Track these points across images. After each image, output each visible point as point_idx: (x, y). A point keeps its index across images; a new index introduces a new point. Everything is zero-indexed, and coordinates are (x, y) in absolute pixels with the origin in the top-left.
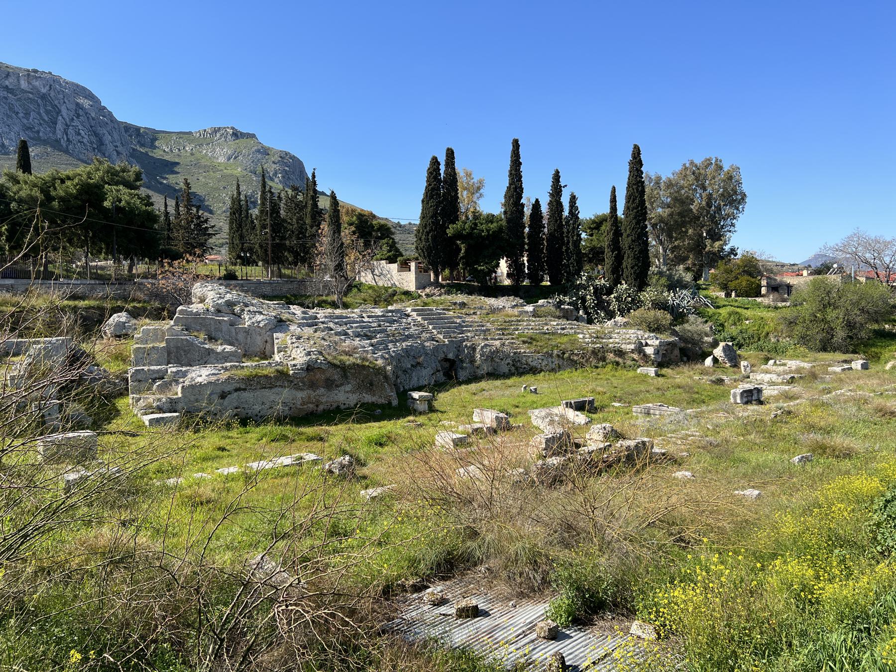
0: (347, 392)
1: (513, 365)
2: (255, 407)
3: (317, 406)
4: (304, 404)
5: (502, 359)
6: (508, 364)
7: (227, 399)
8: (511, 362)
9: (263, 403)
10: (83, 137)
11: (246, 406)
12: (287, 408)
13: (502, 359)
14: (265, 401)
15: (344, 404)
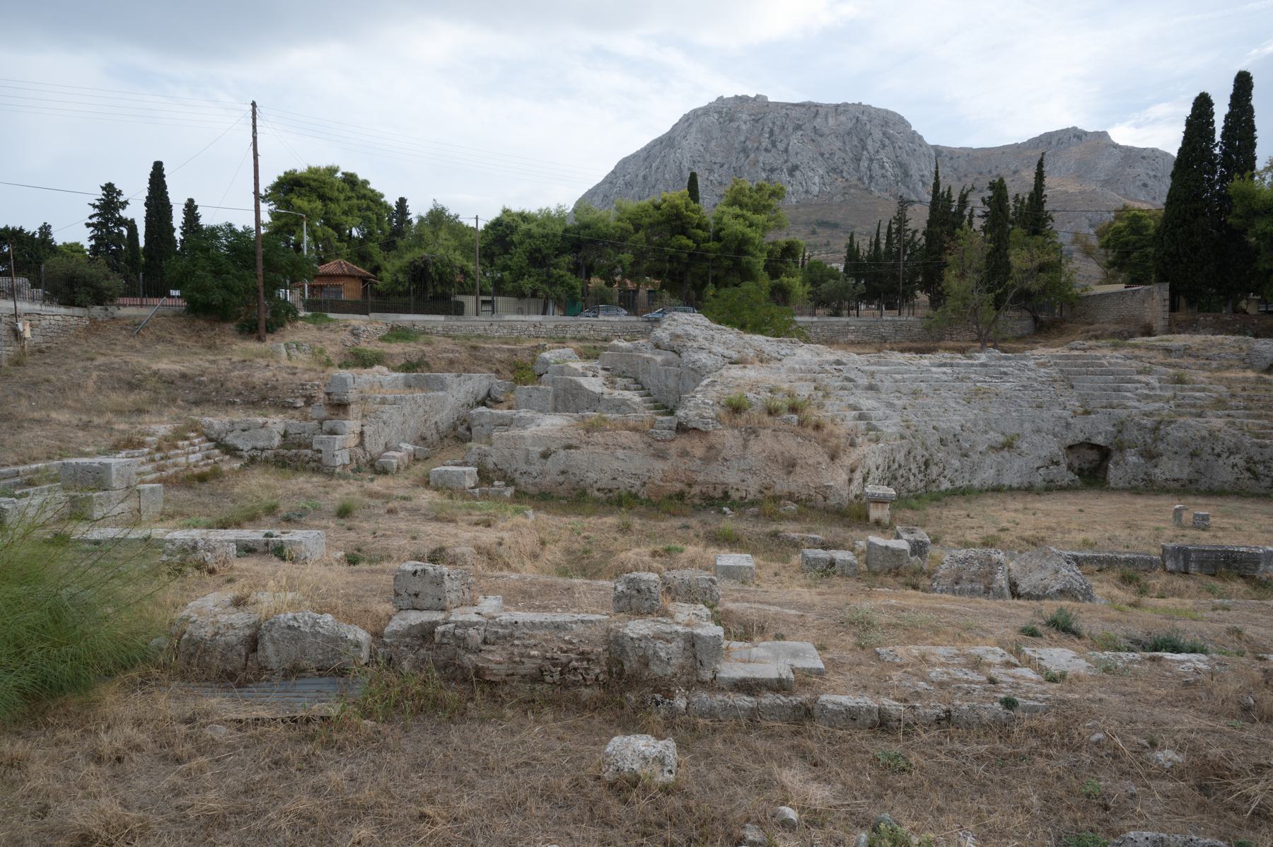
0: (743, 471)
1: (1249, 470)
2: (589, 474)
3: (690, 485)
4: (666, 481)
5: (1219, 455)
6: (1234, 466)
7: (550, 459)
8: (1241, 463)
9: (601, 470)
10: (887, 171)
11: (577, 472)
12: (638, 483)
13: (1219, 455)
14: (604, 468)
15: (737, 490)
